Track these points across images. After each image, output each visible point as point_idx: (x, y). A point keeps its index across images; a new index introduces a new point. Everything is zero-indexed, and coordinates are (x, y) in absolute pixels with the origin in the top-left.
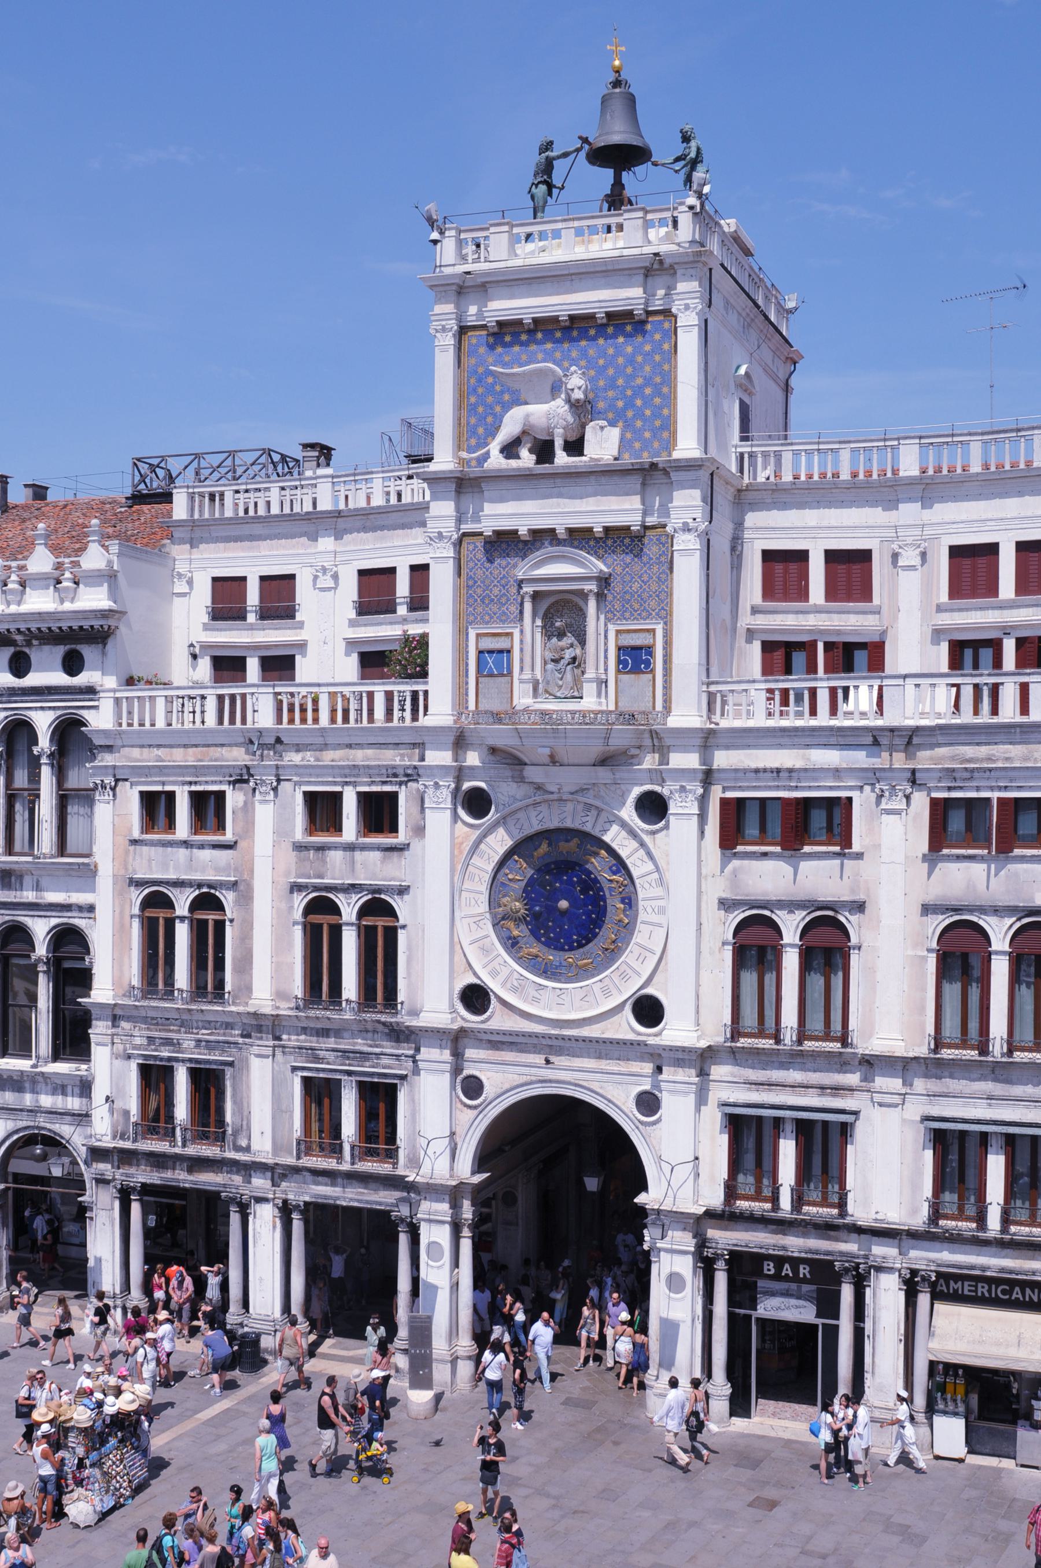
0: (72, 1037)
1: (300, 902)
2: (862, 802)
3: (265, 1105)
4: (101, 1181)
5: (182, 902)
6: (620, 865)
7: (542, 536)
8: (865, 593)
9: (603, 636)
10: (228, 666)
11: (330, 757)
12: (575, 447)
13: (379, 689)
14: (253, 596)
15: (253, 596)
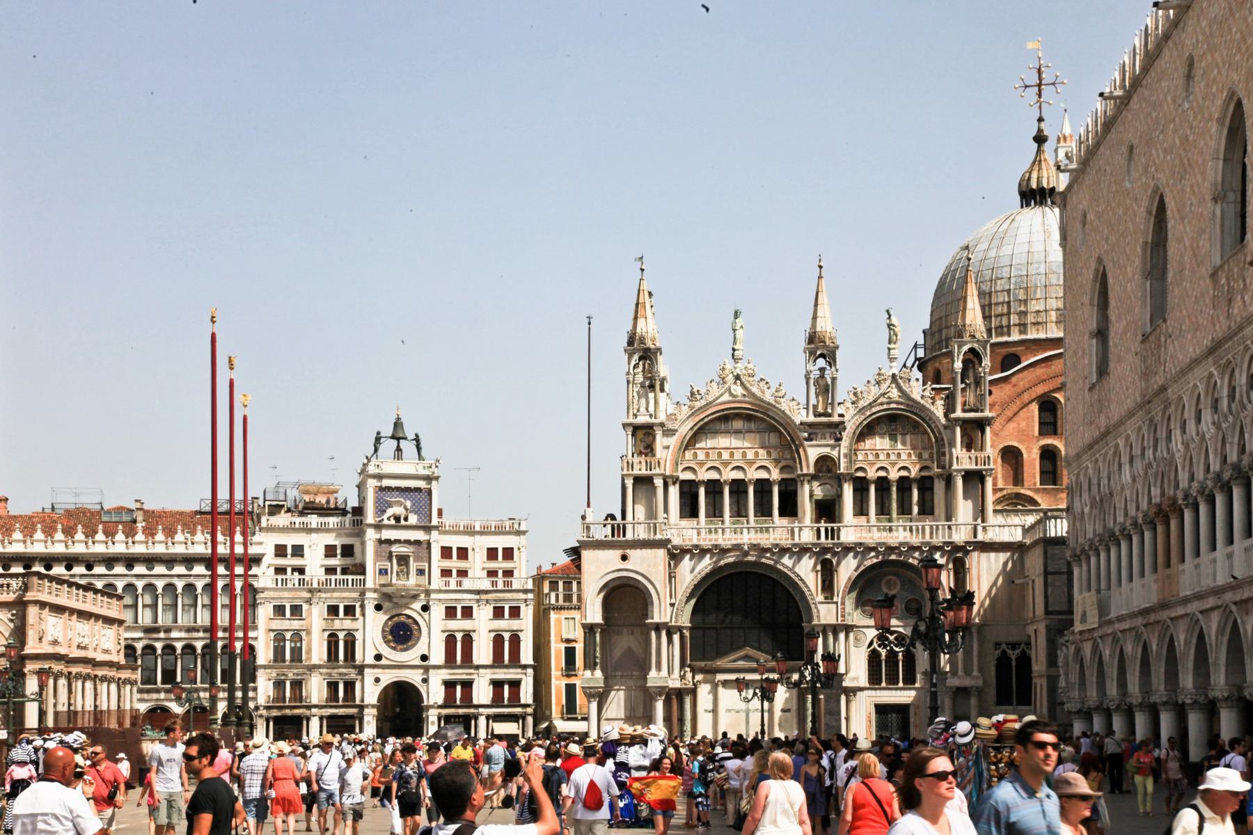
0: (250, 675)
1: (327, 634)
2: (475, 606)
3: (316, 689)
4: (261, 716)
5: (288, 635)
6: (416, 623)
7: (398, 541)
8: (466, 558)
9: (413, 566)
10: (280, 570)
11: (336, 595)
12: (406, 519)
13: (350, 577)
14: (289, 551)
15: (289, 551)
